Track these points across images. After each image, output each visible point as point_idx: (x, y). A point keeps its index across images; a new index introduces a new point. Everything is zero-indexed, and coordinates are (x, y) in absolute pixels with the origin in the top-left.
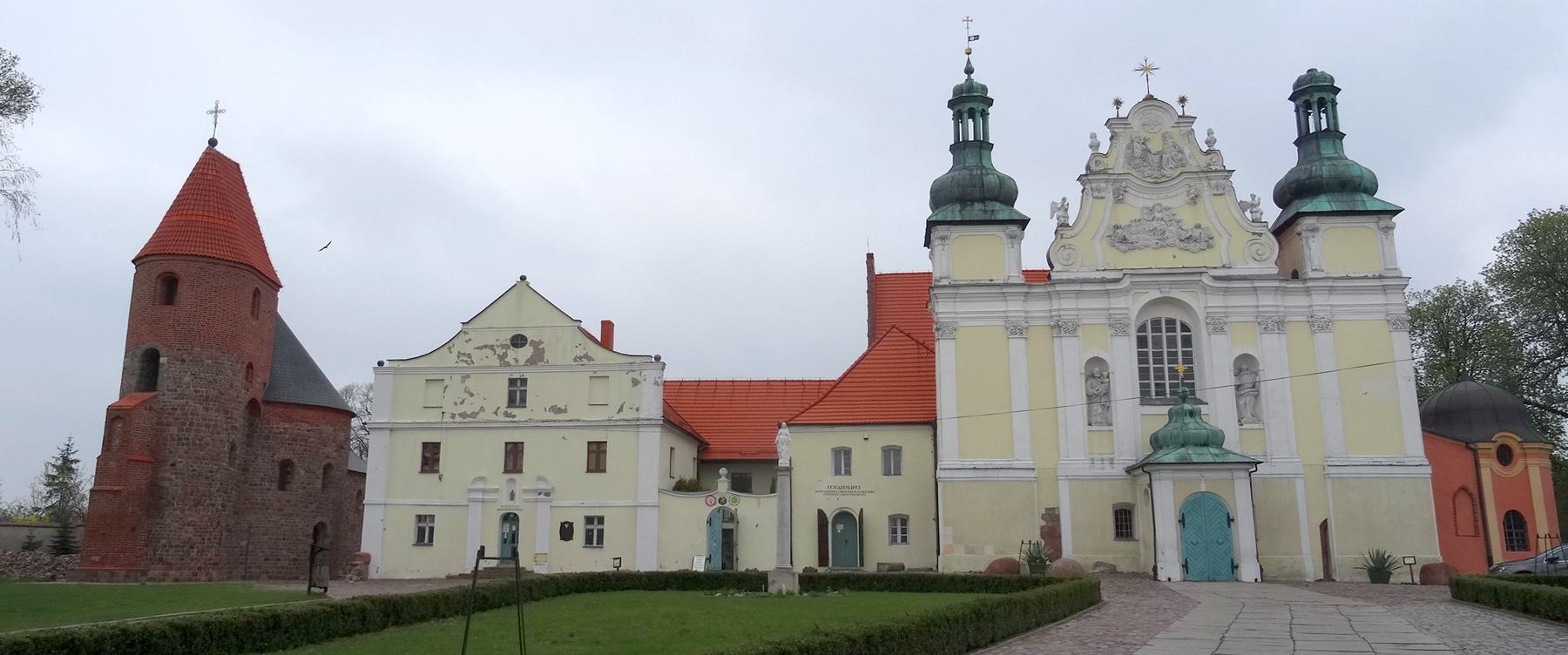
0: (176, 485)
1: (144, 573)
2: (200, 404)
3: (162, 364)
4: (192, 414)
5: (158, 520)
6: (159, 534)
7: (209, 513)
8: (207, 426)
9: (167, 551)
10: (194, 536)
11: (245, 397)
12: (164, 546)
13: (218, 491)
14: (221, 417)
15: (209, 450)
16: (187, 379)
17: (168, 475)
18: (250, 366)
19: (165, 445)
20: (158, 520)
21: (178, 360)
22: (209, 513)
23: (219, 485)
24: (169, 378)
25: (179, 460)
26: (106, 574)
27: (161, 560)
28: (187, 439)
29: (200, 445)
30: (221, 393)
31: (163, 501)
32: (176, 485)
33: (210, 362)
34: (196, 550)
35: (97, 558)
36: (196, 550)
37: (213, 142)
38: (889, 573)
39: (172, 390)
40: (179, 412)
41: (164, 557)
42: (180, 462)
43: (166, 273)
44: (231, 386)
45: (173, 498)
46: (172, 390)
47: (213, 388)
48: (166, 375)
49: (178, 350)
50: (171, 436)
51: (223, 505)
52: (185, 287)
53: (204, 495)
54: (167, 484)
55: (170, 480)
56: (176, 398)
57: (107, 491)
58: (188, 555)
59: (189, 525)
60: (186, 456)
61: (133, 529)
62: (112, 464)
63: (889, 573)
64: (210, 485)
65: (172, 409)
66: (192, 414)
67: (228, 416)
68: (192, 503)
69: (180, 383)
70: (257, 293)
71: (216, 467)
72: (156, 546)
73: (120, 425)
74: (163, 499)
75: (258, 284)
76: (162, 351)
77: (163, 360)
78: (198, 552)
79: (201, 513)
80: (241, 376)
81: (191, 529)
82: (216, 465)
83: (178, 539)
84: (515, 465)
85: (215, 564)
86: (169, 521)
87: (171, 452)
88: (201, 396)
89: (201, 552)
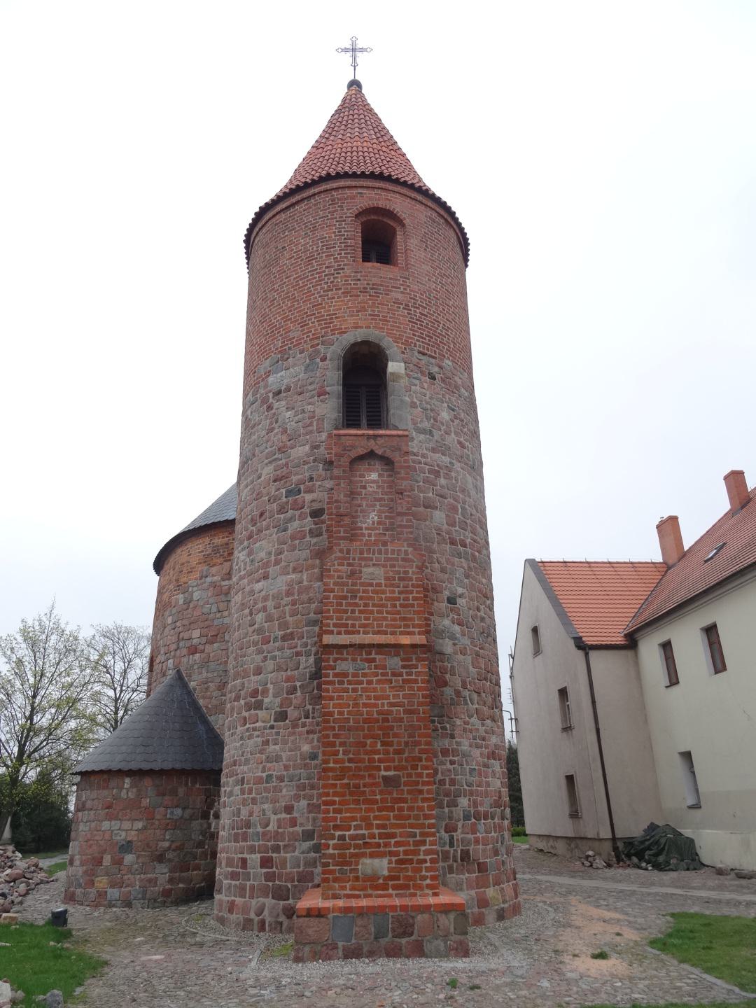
5: (446, 743)
6: (453, 782)
9: (474, 832)
16: (445, 415)
17: (447, 622)
19: (432, 551)
20: (446, 743)
21: (422, 373)
24: (413, 405)
26: (447, 921)
27: (466, 856)
31: (448, 691)
32: (463, 652)
35: (381, 866)
38: (342, 823)
39: (423, 431)
40: (442, 481)
41: (471, 848)
42: (461, 596)
45: (464, 685)
46: (423, 431)
48: (407, 398)
49: (420, 352)
50: (439, 530)
52: (413, 242)
54: (448, 647)
55: (453, 637)
56: (434, 450)
57: (380, 647)
60: (466, 580)
63: (342, 823)
66: (463, 491)
69: (435, 420)
72: (450, 818)
73: (374, 476)
74: (445, 684)
76: (392, 348)
77: (394, 367)
83: (486, 794)
84: (719, 666)
87: (443, 570)
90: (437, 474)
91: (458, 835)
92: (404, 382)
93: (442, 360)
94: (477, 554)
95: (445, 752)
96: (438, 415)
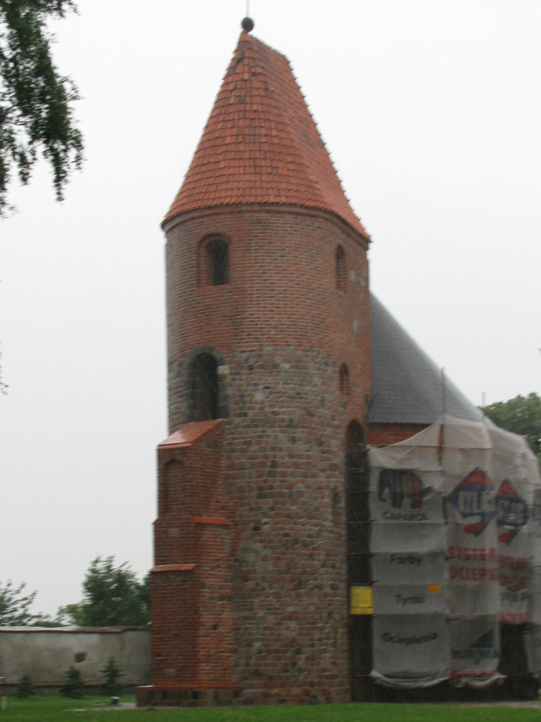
0: (265, 559)
1: (237, 693)
2: (283, 432)
3: (224, 376)
4: (273, 449)
5: (246, 613)
6: (250, 634)
7: (315, 600)
8: (296, 465)
10: (300, 635)
11: (343, 421)
12: (260, 651)
13: (323, 566)
14: (315, 451)
15: (304, 503)
18: (344, 371)
22: (315, 600)
23: (322, 557)
25: (265, 520)
28: (271, 488)
29: (290, 496)
30: (311, 414)
33: (287, 366)
34: (303, 656)
36: (303, 656)
37: (248, 25)
40: (254, 447)
43: (211, 235)
44: (323, 401)
47: (298, 407)
51: (333, 587)
53: (305, 573)
54: (251, 558)
55: (256, 551)
56: (249, 426)
58: (294, 664)
59: (290, 618)
61: (215, 627)
62: (174, 531)
64: (311, 557)
65: (245, 443)
66: (273, 449)
67: (324, 448)
68: (290, 585)
70: (340, 253)
71: (317, 528)
75: (340, 239)
77: (223, 370)
78: (307, 659)
79: (305, 599)
80: (334, 385)
81: (293, 625)
82: (316, 525)
83: (277, 640)
85: (333, 677)
86: (261, 614)
87: (251, 509)
88: (283, 420)
89: (311, 659)
90: (250, 443)
91: (253, 661)
92: (229, 379)
93: (261, 350)
94: (286, 491)
95: (246, 618)
96: (254, 397)
